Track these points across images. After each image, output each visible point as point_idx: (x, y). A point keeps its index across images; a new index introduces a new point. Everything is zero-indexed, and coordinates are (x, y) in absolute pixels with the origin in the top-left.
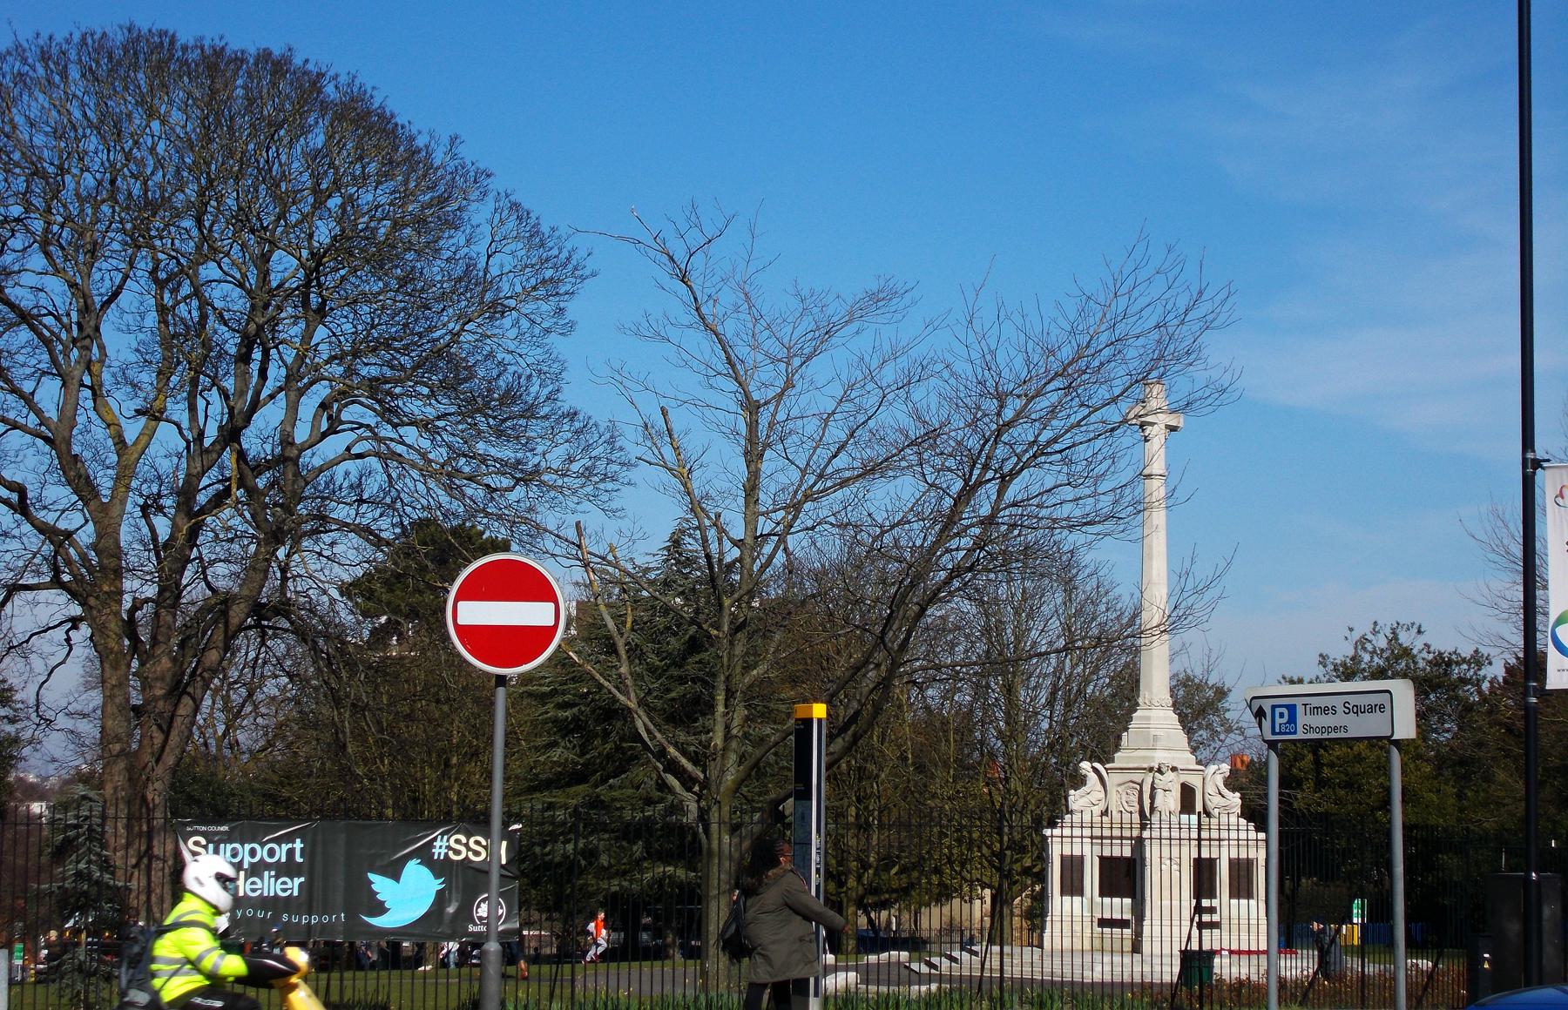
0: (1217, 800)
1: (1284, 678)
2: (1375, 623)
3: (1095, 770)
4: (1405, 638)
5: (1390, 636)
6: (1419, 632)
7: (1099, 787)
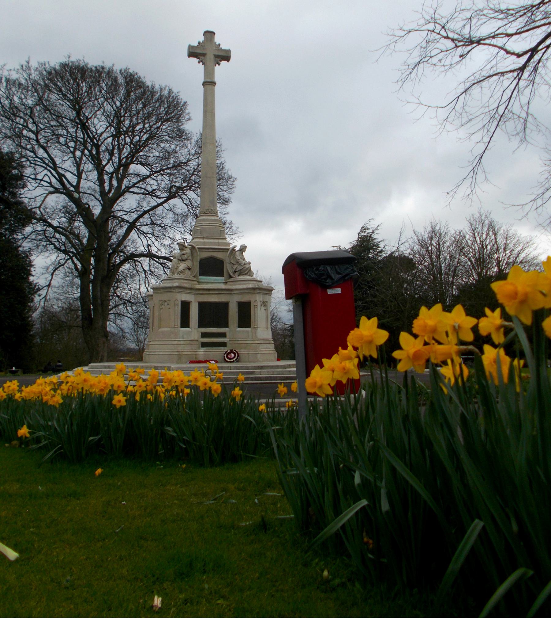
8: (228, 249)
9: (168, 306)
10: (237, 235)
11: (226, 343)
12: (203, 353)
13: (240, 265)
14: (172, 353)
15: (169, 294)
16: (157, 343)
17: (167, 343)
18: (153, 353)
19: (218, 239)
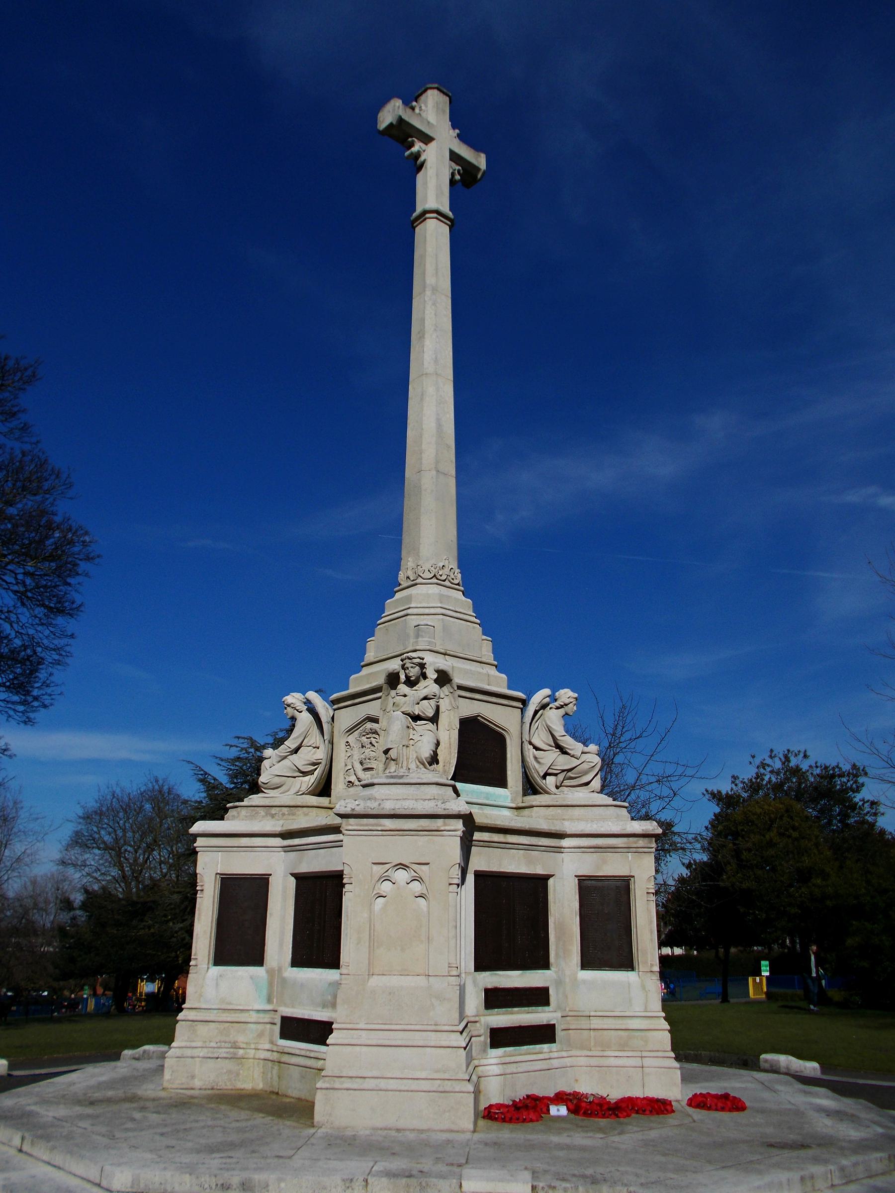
0: (551, 757)
1: (707, 791)
2: (772, 751)
3: (312, 711)
4: (793, 762)
5: (783, 759)
6: (805, 756)
7: (315, 737)
9: (416, 887)
10: (49, 690)
11: (554, 1025)
12: (496, 1070)
13: (563, 751)
14: (448, 1086)
15: (422, 840)
16: (364, 1037)
17: (418, 1038)
18: (348, 1084)
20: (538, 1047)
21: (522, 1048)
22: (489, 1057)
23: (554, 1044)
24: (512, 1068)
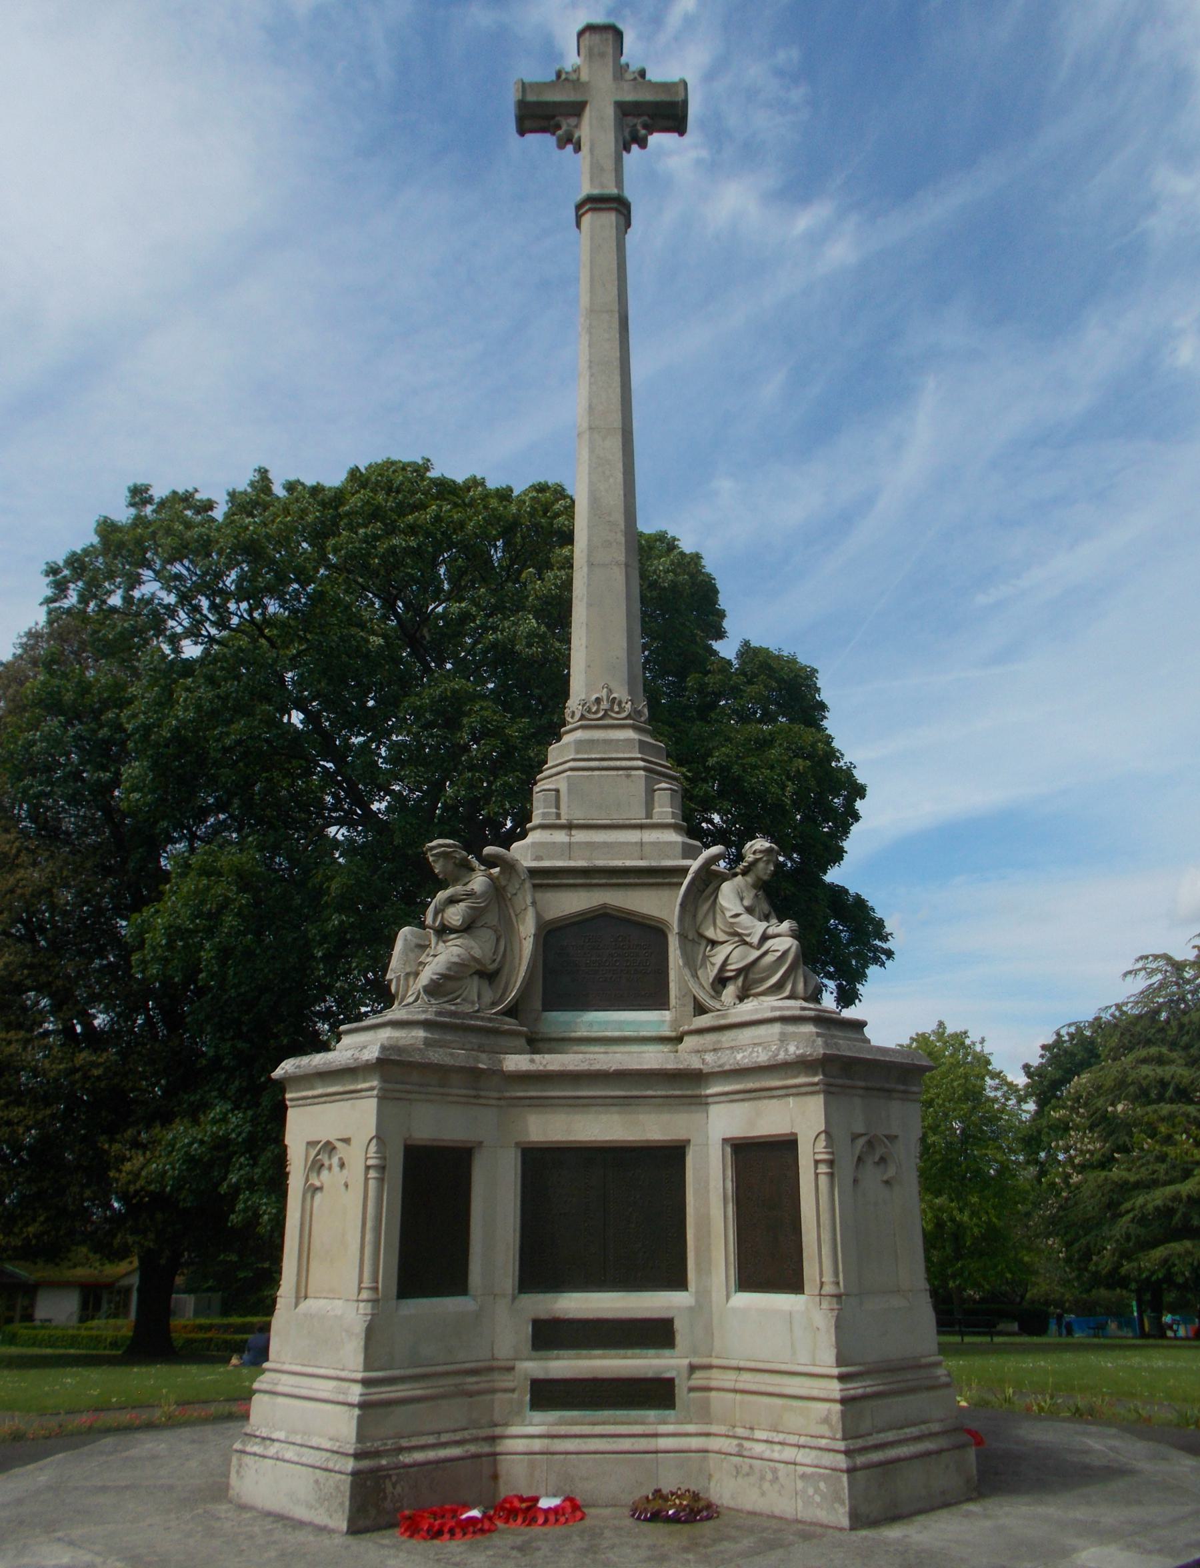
8: (685, 870)
11: (671, 1381)
19: (641, 827)
20: (634, 1414)
21: (600, 1413)
22: (527, 1423)
23: (672, 1412)
24: (570, 1445)
